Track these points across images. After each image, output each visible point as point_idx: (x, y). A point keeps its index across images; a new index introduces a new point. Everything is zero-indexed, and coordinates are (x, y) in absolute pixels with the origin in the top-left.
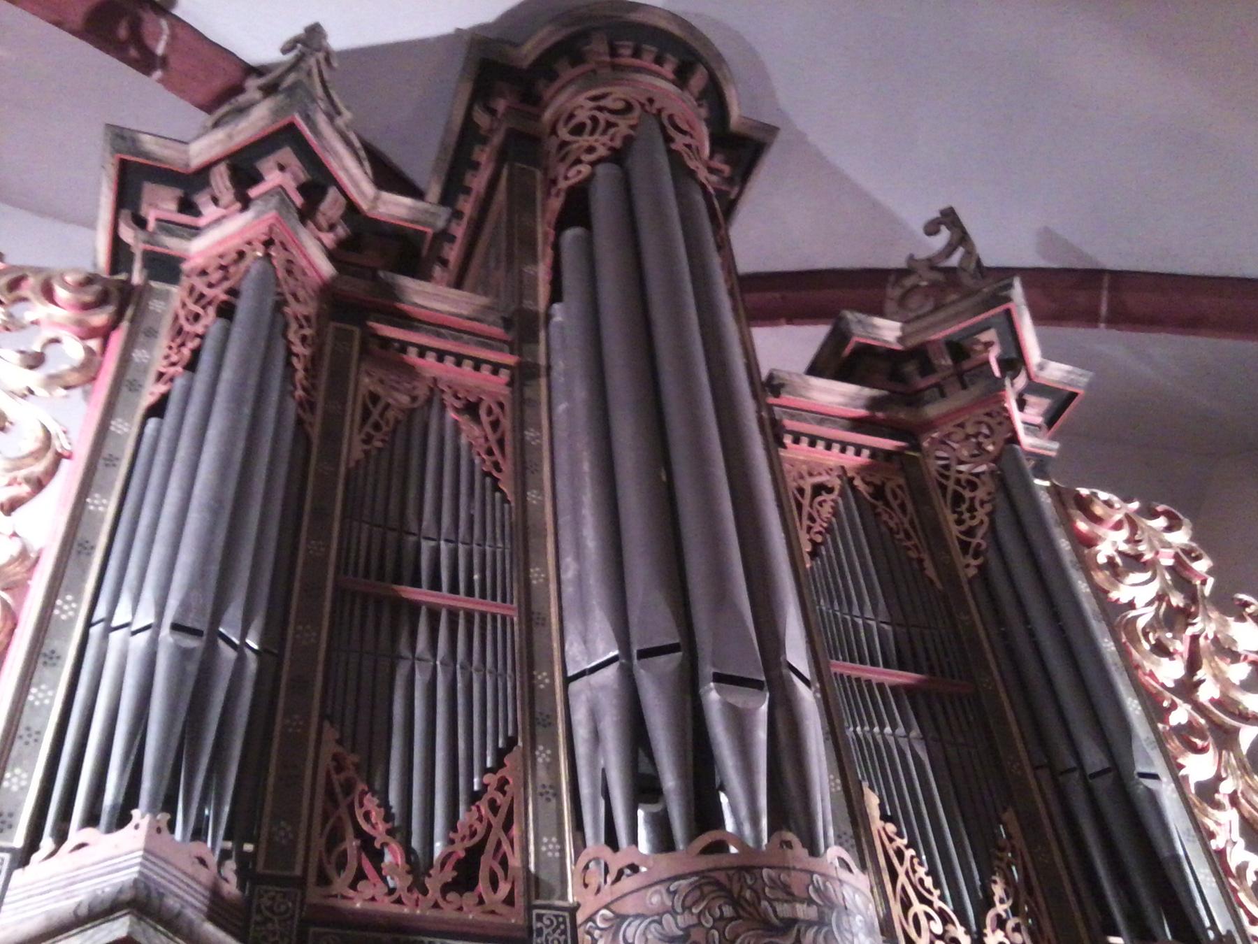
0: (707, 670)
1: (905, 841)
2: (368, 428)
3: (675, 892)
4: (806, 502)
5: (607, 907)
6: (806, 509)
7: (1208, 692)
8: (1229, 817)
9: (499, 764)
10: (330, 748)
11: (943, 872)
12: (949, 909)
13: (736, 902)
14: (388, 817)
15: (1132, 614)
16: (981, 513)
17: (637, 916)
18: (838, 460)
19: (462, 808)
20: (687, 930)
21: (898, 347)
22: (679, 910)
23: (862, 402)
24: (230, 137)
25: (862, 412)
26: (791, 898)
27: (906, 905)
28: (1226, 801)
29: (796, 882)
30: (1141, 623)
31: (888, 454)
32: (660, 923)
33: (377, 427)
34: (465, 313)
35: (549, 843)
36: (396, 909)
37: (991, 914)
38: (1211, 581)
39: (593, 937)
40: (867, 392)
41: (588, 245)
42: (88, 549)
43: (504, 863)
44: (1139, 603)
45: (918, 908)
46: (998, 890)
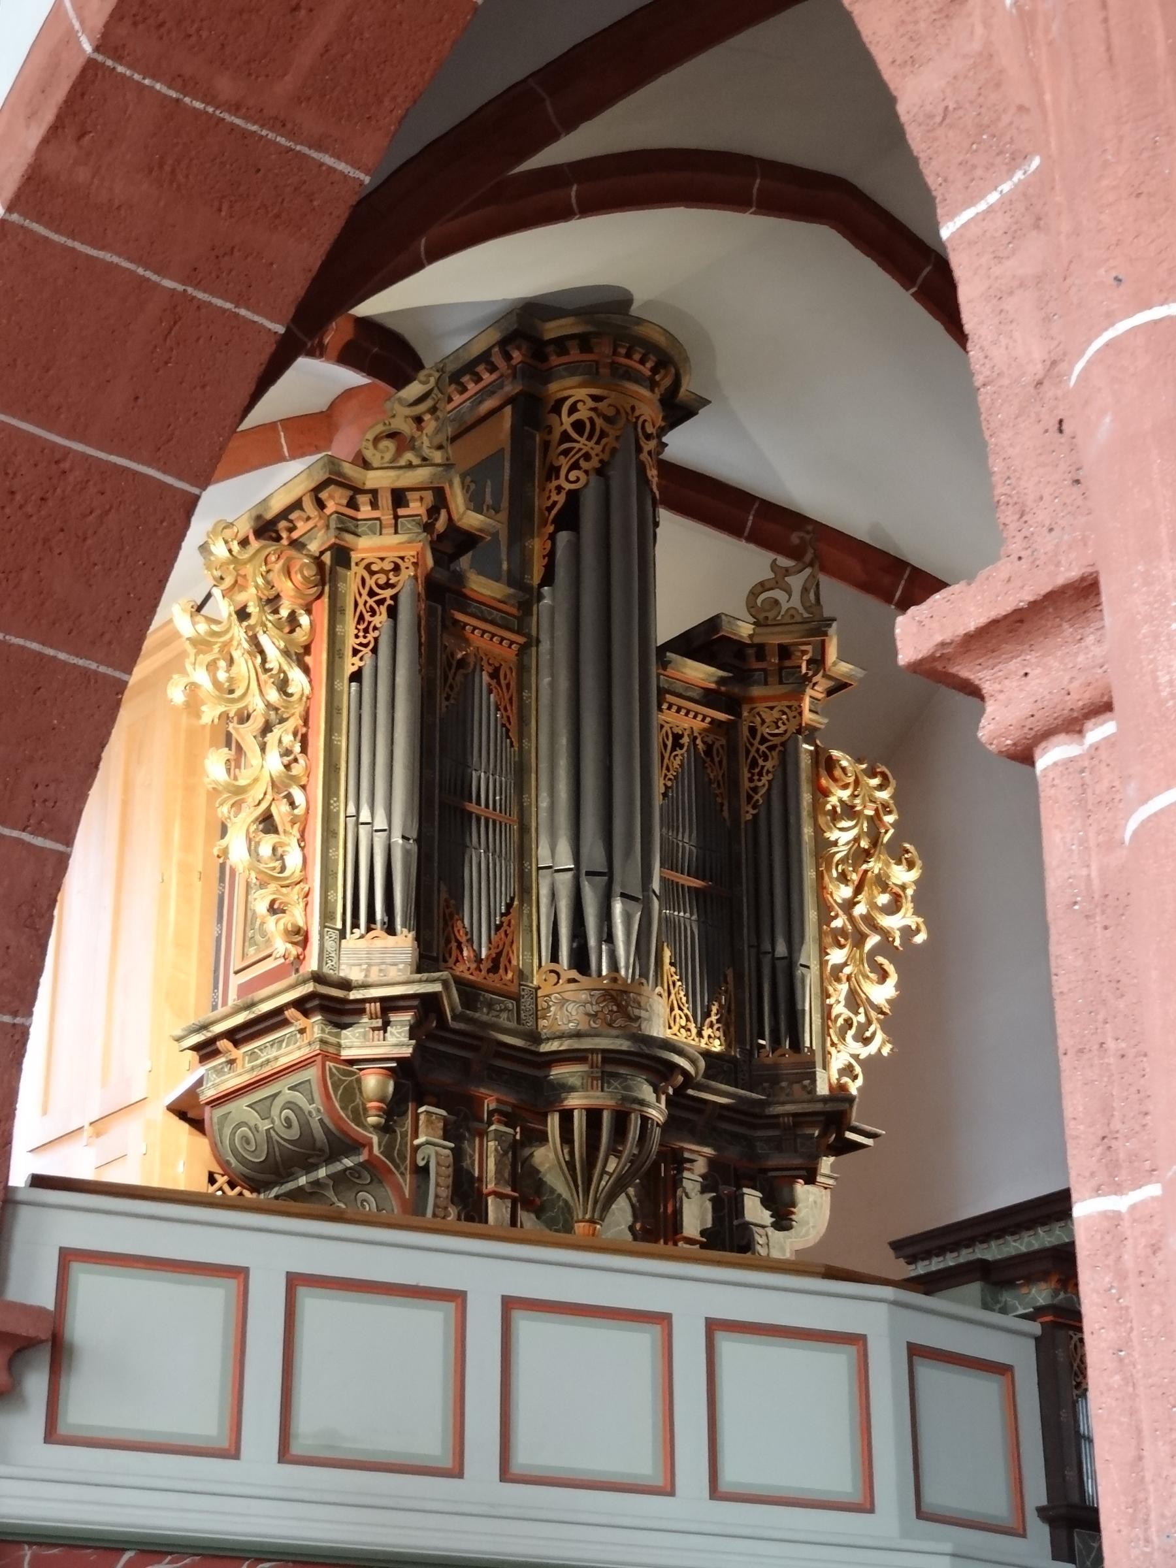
0: (617, 889)
2: (447, 689)
4: (667, 755)
6: (666, 761)
7: (860, 910)
8: (844, 988)
9: (508, 913)
10: (444, 895)
11: (691, 995)
12: (690, 1014)
13: (619, 1005)
14: (466, 934)
15: (835, 849)
16: (765, 779)
18: (689, 721)
19: (493, 932)
20: (597, 1012)
21: (748, 641)
23: (715, 679)
24: (398, 477)
25: (713, 686)
27: (672, 1009)
28: (844, 979)
29: (643, 1001)
30: (838, 857)
31: (721, 723)
33: (451, 687)
34: (499, 597)
35: (528, 954)
36: (471, 977)
37: (708, 1020)
38: (891, 831)
40: (721, 673)
41: (576, 550)
42: (337, 770)
43: (510, 962)
44: (841, 842)
45: (677, 1011)
46: (714, 1009)
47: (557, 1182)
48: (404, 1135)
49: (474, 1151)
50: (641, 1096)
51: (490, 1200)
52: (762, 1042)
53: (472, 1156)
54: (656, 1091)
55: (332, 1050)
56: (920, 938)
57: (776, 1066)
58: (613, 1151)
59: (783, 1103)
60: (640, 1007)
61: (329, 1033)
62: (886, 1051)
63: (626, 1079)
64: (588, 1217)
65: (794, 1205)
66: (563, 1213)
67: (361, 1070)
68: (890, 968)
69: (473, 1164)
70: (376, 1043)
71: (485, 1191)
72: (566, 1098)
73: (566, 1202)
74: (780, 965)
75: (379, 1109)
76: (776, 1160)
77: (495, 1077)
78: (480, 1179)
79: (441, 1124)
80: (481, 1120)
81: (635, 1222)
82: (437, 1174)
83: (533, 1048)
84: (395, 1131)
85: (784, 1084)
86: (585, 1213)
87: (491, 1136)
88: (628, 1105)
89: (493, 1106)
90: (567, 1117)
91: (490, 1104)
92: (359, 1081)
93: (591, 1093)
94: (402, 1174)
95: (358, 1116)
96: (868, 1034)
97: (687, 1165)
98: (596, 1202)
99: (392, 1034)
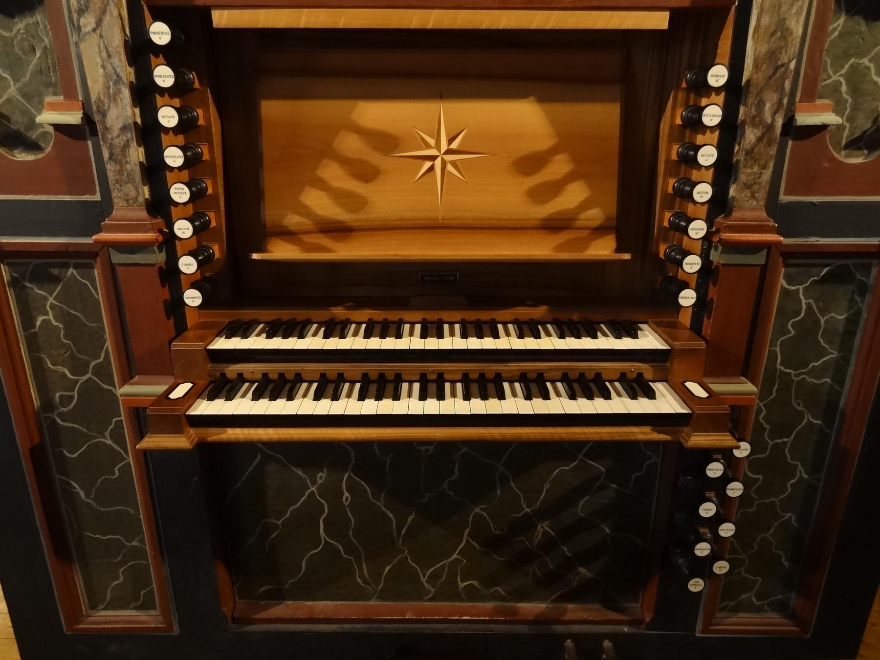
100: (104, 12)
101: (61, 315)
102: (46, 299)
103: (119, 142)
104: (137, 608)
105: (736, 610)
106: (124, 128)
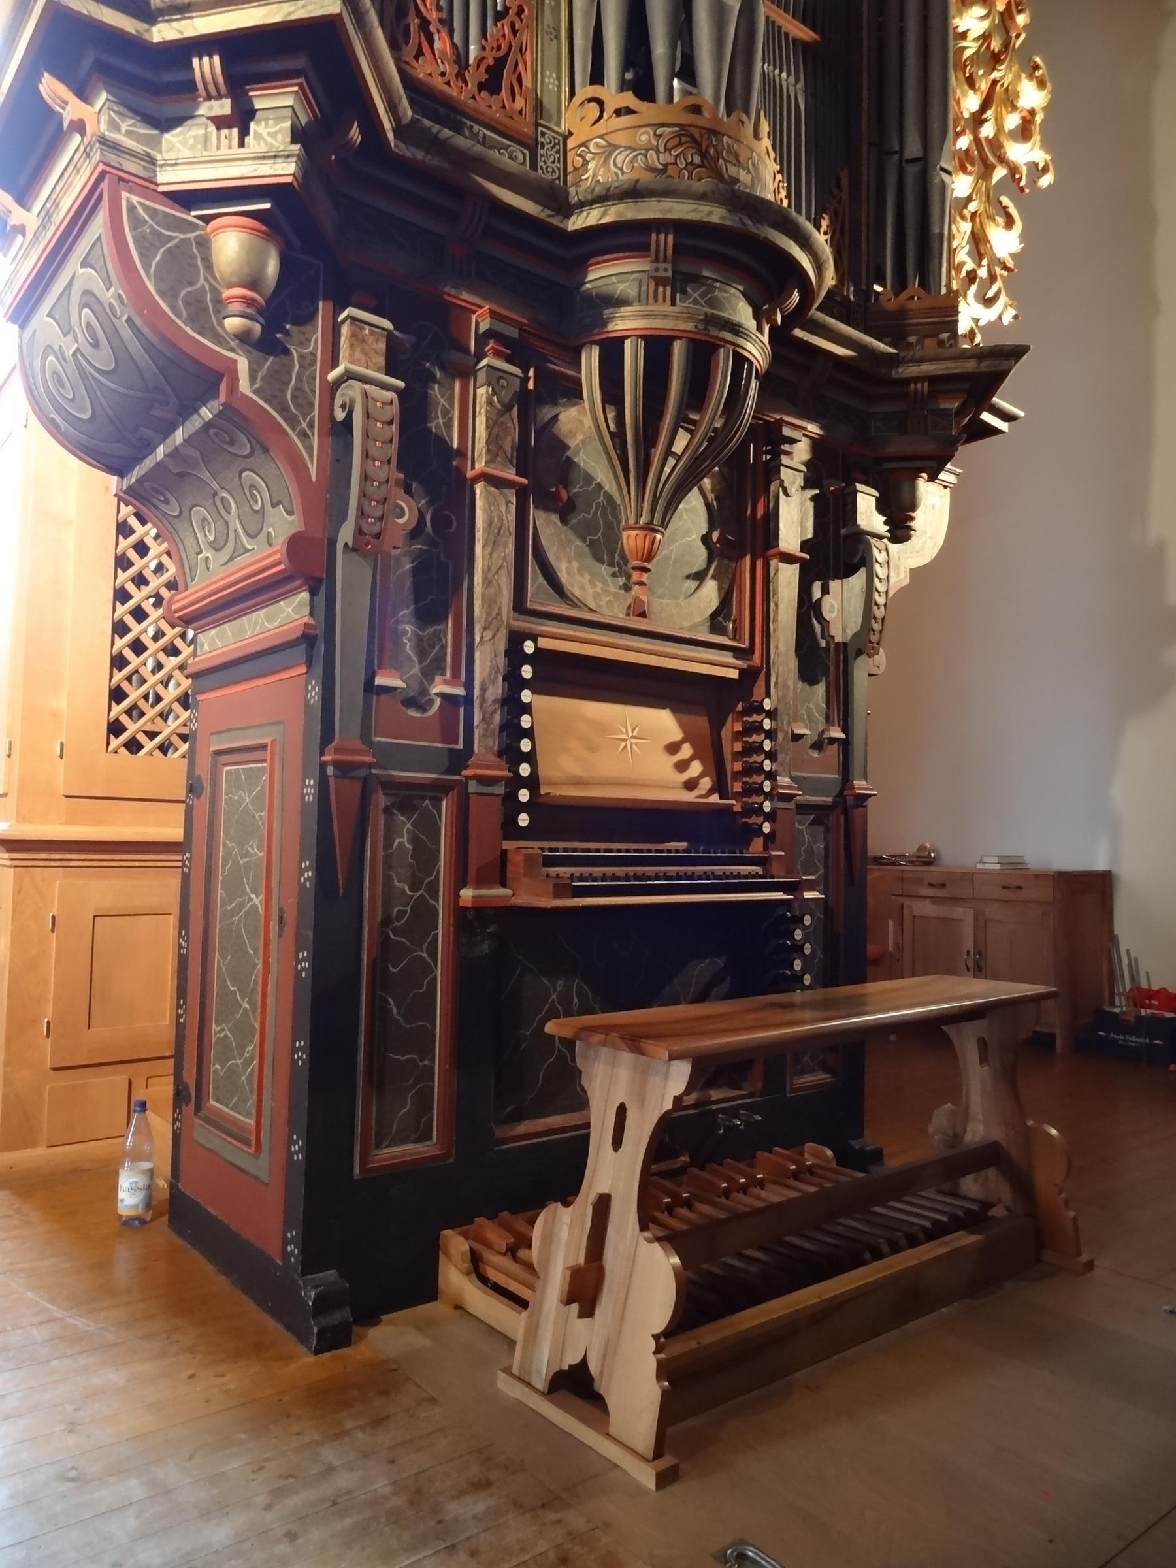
1: (778, 168)
3: (660, 136)
5: (601, 137)
7: (987, 130)
8: (966, 227)
13: (703, 155)
15: (964, 44)
17: (627, 148)
19: (490, 22)
20: (666, 165)
22: (662, 150)
26: (738, 162)
28: (968, 216)
30: (967, 53)
32: (646, 156)
36: (446, 88)
38: (1023, 36)
39: (584, 159)
44: (972, 35)
47: (595, 464)
48: (308, 362)
49: (452, 403)
50: (735, 318)
51: (479, 488)
52: (877, 288)
53: (447, 413)
54: (757, 316)
55: (132, 166)
56: (1046, 181)
57: (902, 313)
58: (681, 420)
59: (920, 361)
60: (738, 162)
61: (129, 133)
62: (1007, 319)
63: (712, 288)
64: (642, 521)
65: (913, 507)
66: (604, 515)
67: (207, 219)
68: (1013, 211)
69: (449, 425)
70: (224, 150)
71: (470, 474)
72: (612, 319)
73: (609, 498)
74: (912, 170)
75: (250, 302)
76: (899, 445)
77: (491, 277)
78: (461, 453)
79: (382, 346)
80: (466, 350)
81: (711, 529)
82: (366, 434)
83: (555, 221)
84: (287, 352)
85: (912, 339)
86: (639, 515)
87: (482, 377)
88: (714, 332)
89: (485, 326)
90: (612, 352)
91: (480, 321)
92: (204, 244)
93: (653, 307)
94: (304, 436)
95: (203, 311)
96: (990, 294)
97: (786, 447)
98: (655, 500)
99: (258, 137)
100: (498, 630)
101: (415, 840)
102: (404, 823)
103: (490, 709)
104: (416, 1141)
105: (802, 1073)
106: (494, 701)
